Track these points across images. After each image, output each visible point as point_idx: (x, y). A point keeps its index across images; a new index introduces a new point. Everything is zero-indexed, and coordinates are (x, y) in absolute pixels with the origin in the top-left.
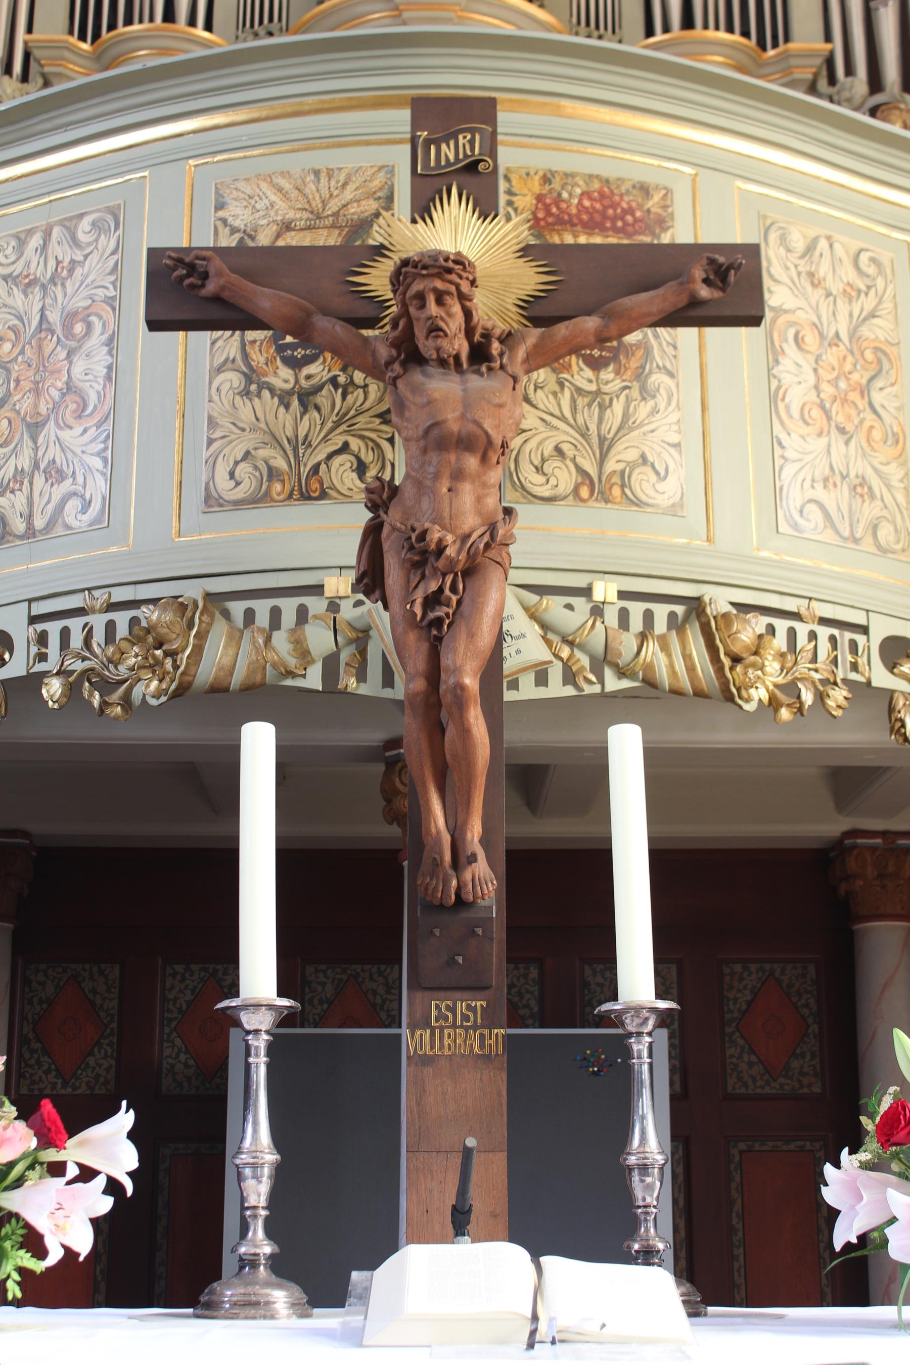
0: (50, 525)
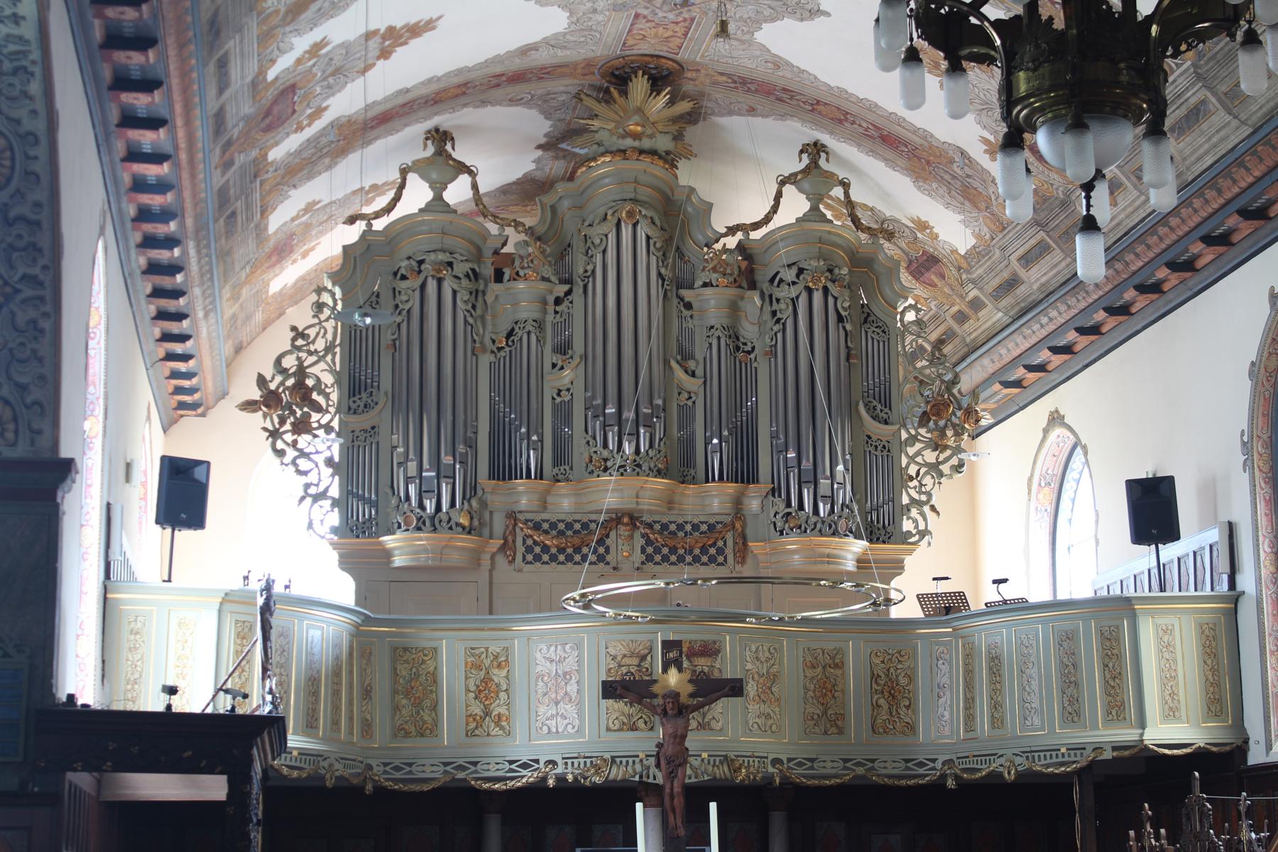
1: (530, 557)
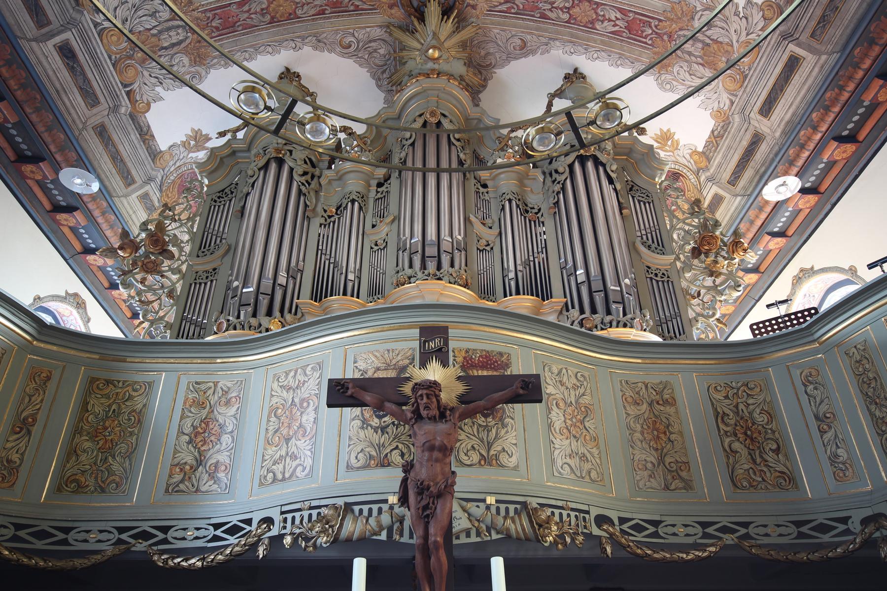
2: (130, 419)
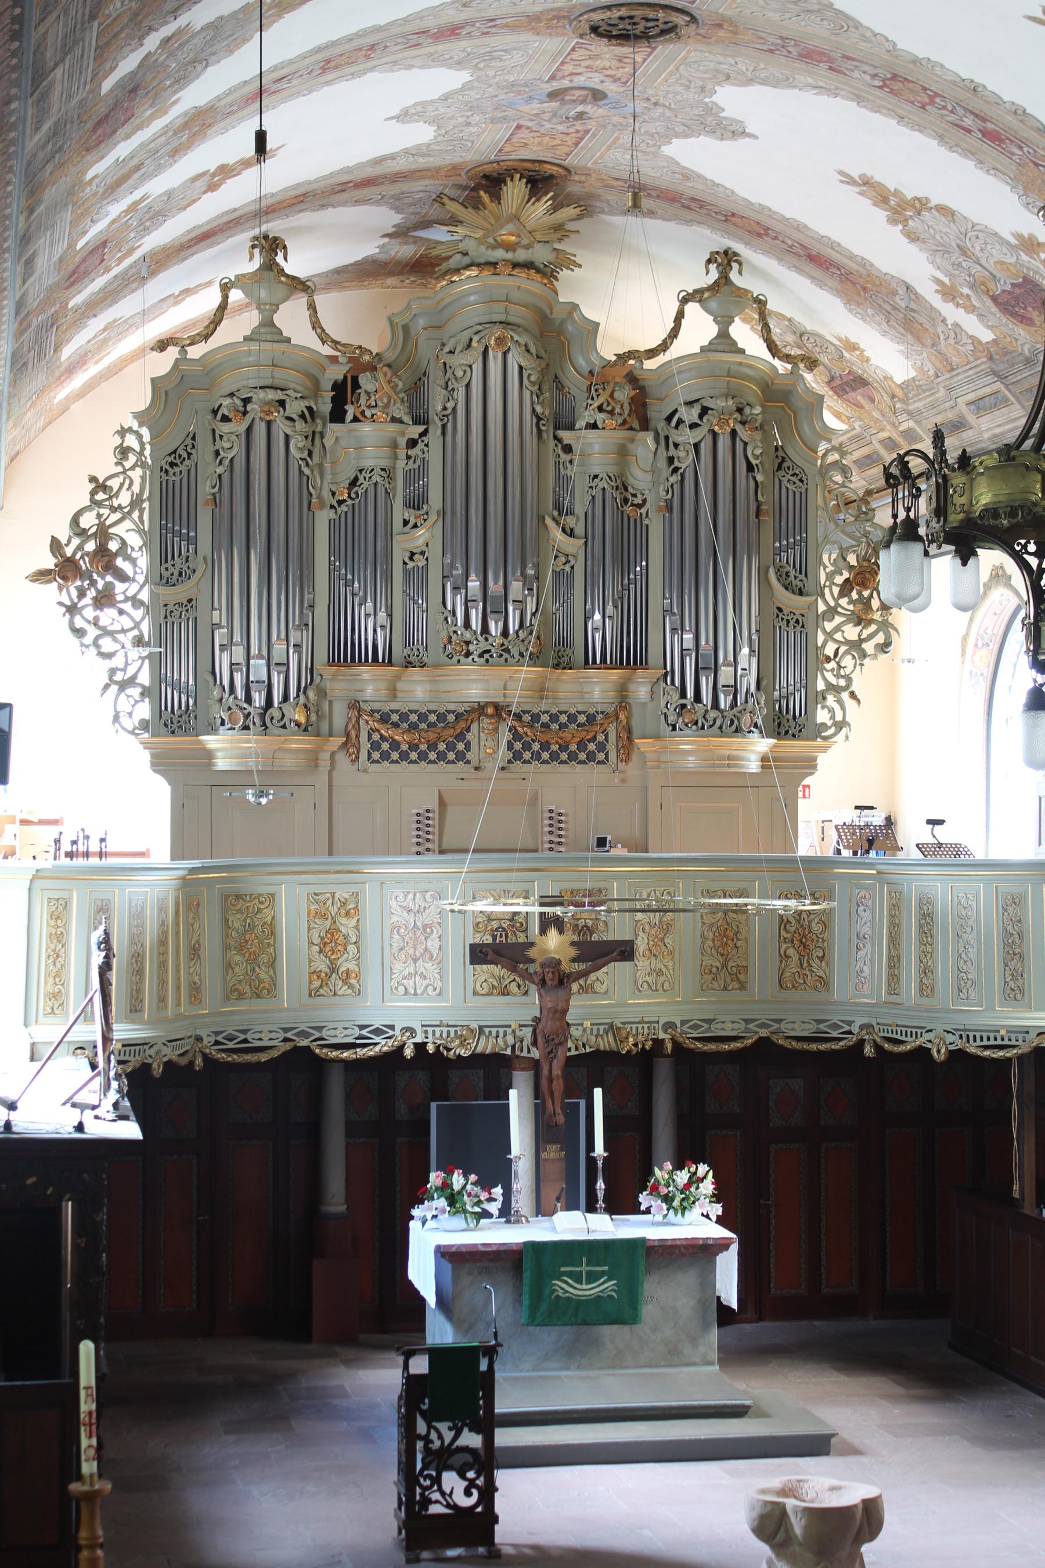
0: (422, 994)
1: (376, 755)
2: (264, 932)
